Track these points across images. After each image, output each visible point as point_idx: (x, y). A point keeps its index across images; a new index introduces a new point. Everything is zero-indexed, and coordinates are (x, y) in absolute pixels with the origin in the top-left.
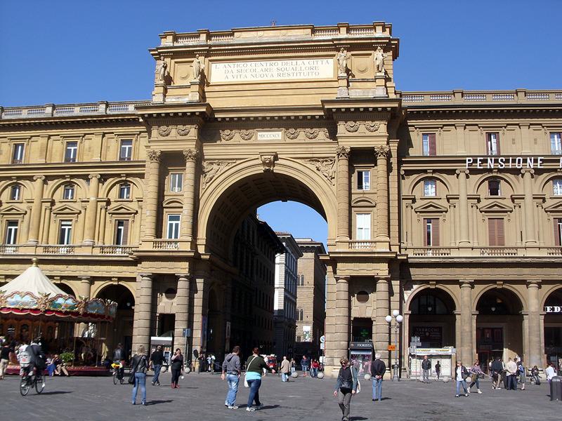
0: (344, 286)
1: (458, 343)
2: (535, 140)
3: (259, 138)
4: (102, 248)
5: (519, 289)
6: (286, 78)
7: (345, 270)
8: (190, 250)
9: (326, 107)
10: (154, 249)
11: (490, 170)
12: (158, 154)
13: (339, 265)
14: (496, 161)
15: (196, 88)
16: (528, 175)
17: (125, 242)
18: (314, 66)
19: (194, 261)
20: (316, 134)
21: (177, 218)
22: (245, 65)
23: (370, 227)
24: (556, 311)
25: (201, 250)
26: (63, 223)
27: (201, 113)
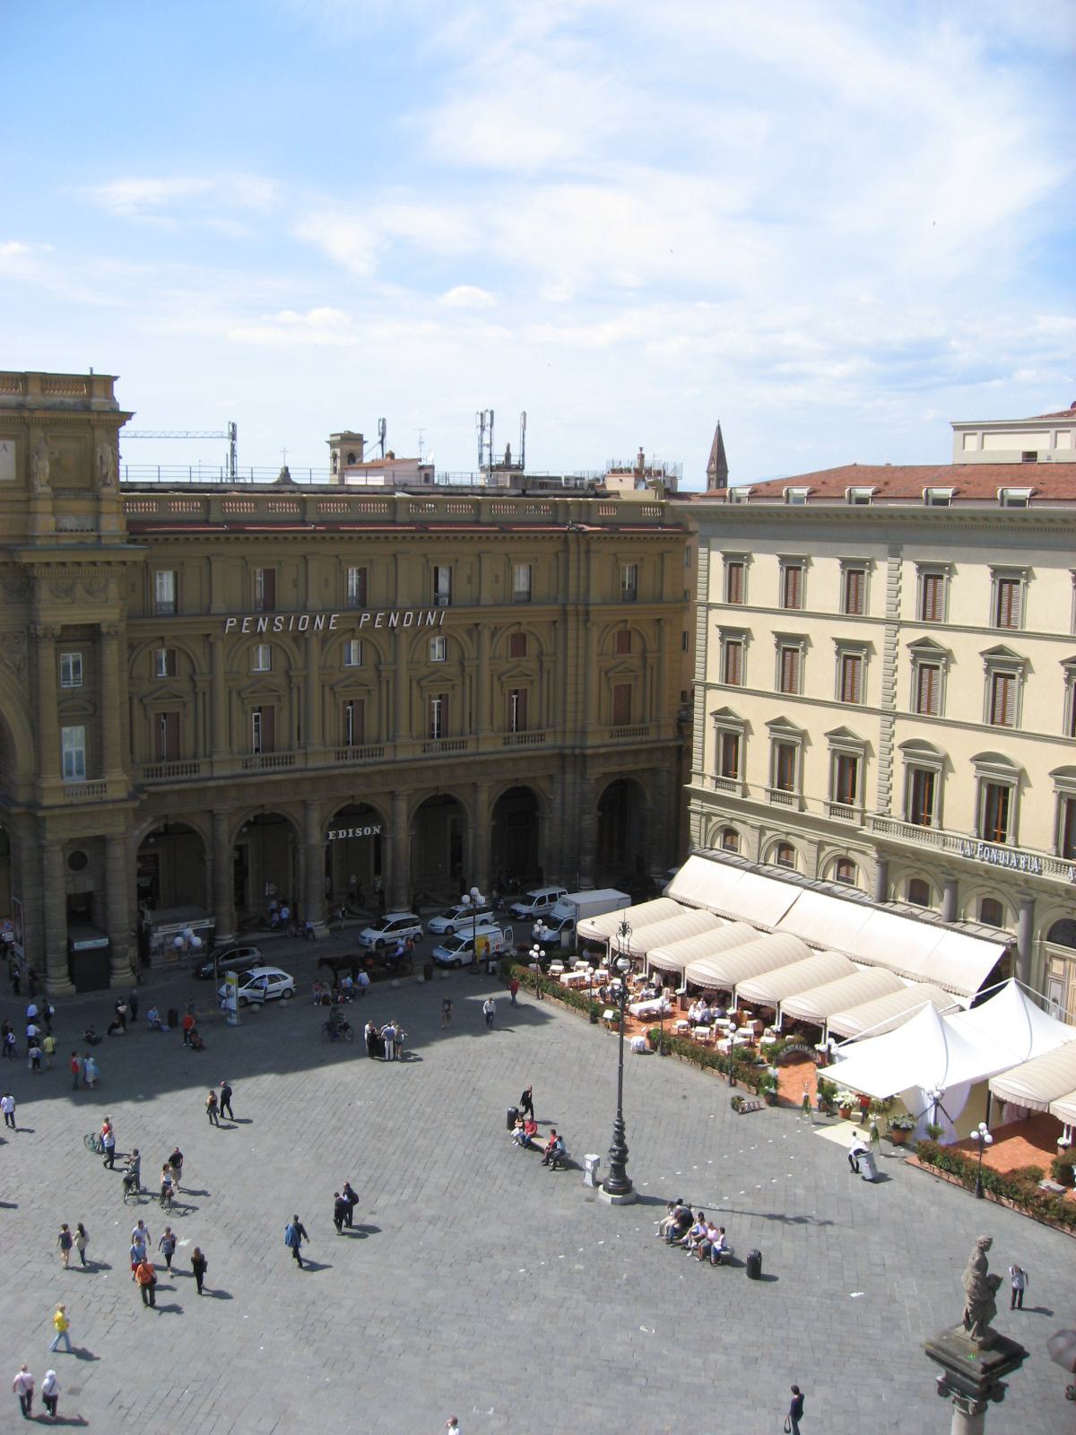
16: (315, 644)
23: (83, 748)
24: (341, 837)
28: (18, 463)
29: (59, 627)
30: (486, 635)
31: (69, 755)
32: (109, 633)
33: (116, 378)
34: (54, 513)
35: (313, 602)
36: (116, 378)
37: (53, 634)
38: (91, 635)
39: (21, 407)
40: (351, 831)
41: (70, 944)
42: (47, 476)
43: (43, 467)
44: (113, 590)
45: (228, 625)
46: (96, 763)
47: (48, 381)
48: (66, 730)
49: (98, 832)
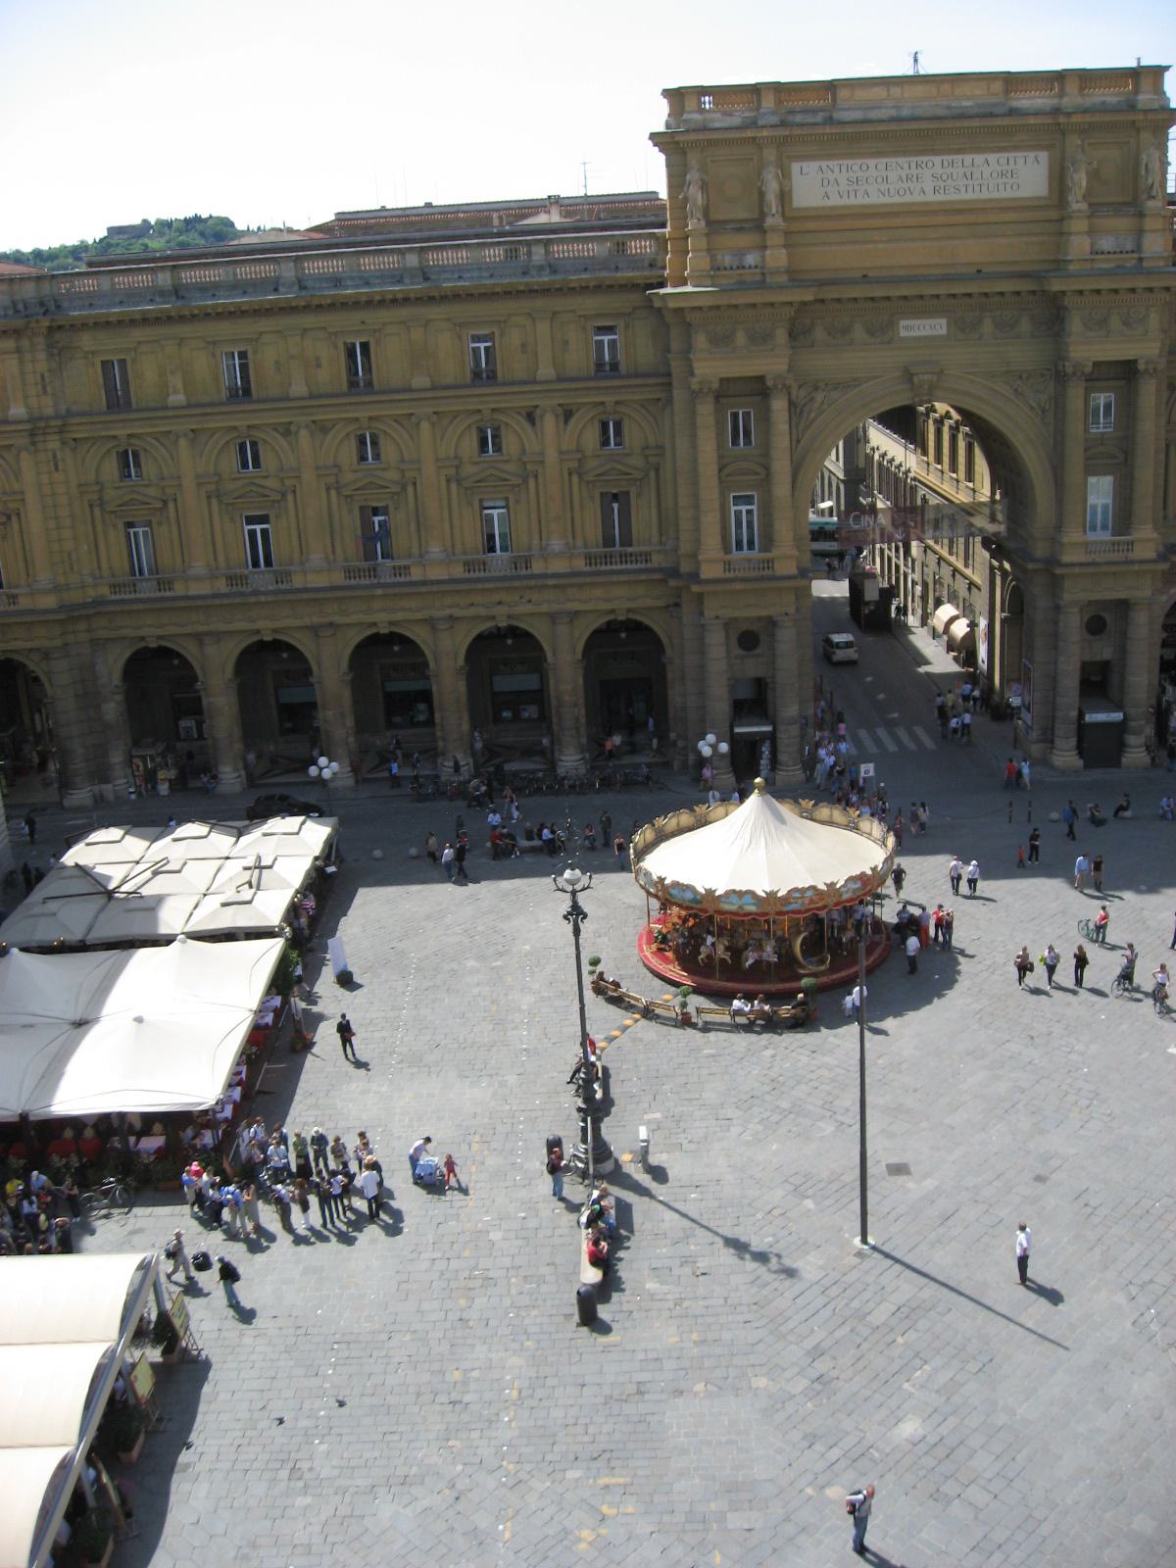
4: (590, 559)
12: (715, 386)
17: (627, 541)
18: (1009, 168)
21: (748, 500)
22: (864, 167)
23: (1109, 501)
26: (486, 504)
28: (1051, 178)
29: (1091, 364)
31: (1094, 508)
32: (1146, 371)
33: (1167, 68)
34: (1091, 232)
36: (1167, 68)
37: (1083, 373)
38: (1126, 373)
39: (1056, 111)
41: (1081, 715)
42: (1083, 190)
43: (1080, 179)
46: (1124, 517)
47: (1086, 78)
48: (1092, 480)
49: (1122, 595)
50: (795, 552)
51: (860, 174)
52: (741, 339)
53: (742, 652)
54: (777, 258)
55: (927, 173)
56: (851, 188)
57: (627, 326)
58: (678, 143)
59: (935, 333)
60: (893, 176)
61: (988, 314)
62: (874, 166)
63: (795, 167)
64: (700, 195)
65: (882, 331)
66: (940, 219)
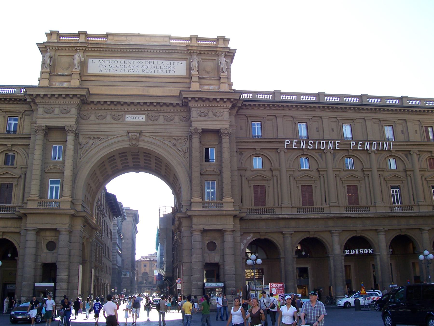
0: (197, 236)
1: (283, 280)
2: (333, 129)
3: (127, 119)
5: (324, 237)
6: (149, 74)
7: (199, 224)
8: (69, 208)
9: (184, 96)
10: (39, 207)
11: (302, 149)
13: (195, 220)
14: (307, 143)
15: (77, 76)
16: (329, 155)
19: (73, 216)
20: (172, 118)
21: (57, 182)
24: (352, 253)
25: (79, 208)
27: (81, 95)
30: (415, 157)
35: (326, 137)
40: (357, 250)
43: (195, 64)
44: (226, 114)
45: (286, 144)
50: (70, 199)
51: (114, 64)
52: (57, 111)
53: (48, 251)
54: (75, 83)
55: (140, 66)
56: (110, 68)
57: (21, 118)
58: (46, 47)
59: (140, 120)
60: (127, 65)
61: (161, 114)
62: (119, 62)
63: (90, 60)
64: (49, 61)
65: (118, 118)
66: (144, 80)
